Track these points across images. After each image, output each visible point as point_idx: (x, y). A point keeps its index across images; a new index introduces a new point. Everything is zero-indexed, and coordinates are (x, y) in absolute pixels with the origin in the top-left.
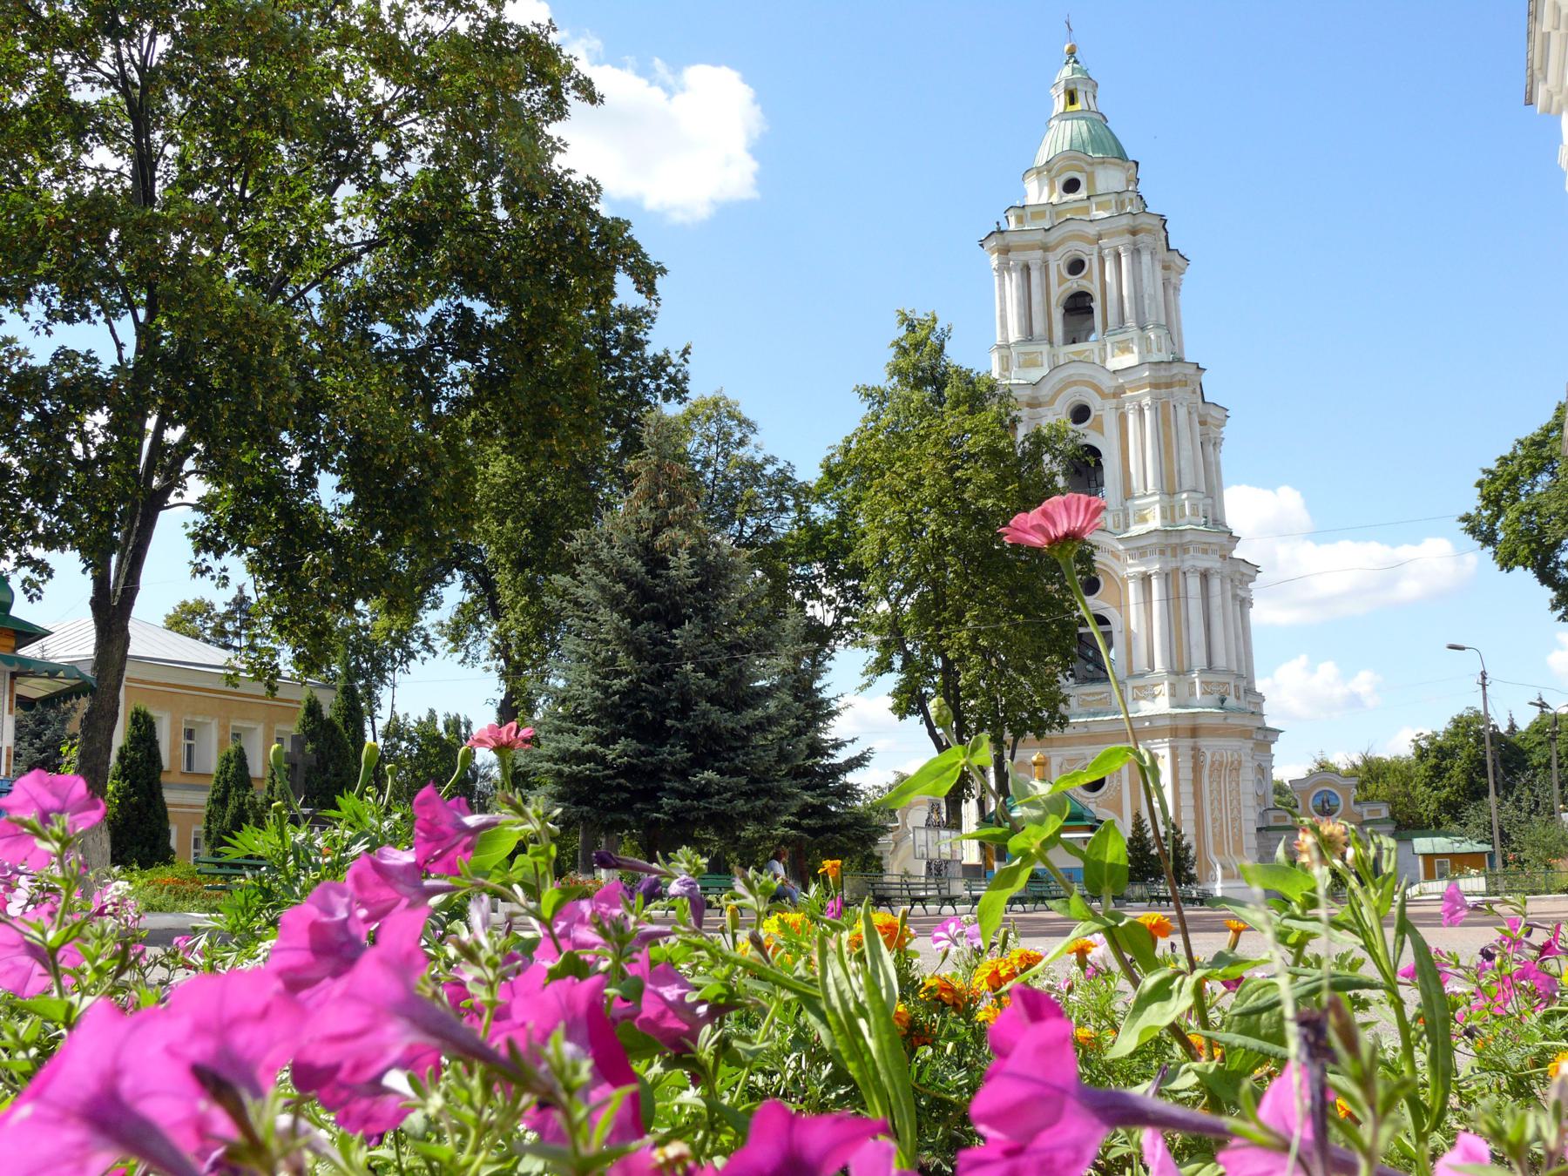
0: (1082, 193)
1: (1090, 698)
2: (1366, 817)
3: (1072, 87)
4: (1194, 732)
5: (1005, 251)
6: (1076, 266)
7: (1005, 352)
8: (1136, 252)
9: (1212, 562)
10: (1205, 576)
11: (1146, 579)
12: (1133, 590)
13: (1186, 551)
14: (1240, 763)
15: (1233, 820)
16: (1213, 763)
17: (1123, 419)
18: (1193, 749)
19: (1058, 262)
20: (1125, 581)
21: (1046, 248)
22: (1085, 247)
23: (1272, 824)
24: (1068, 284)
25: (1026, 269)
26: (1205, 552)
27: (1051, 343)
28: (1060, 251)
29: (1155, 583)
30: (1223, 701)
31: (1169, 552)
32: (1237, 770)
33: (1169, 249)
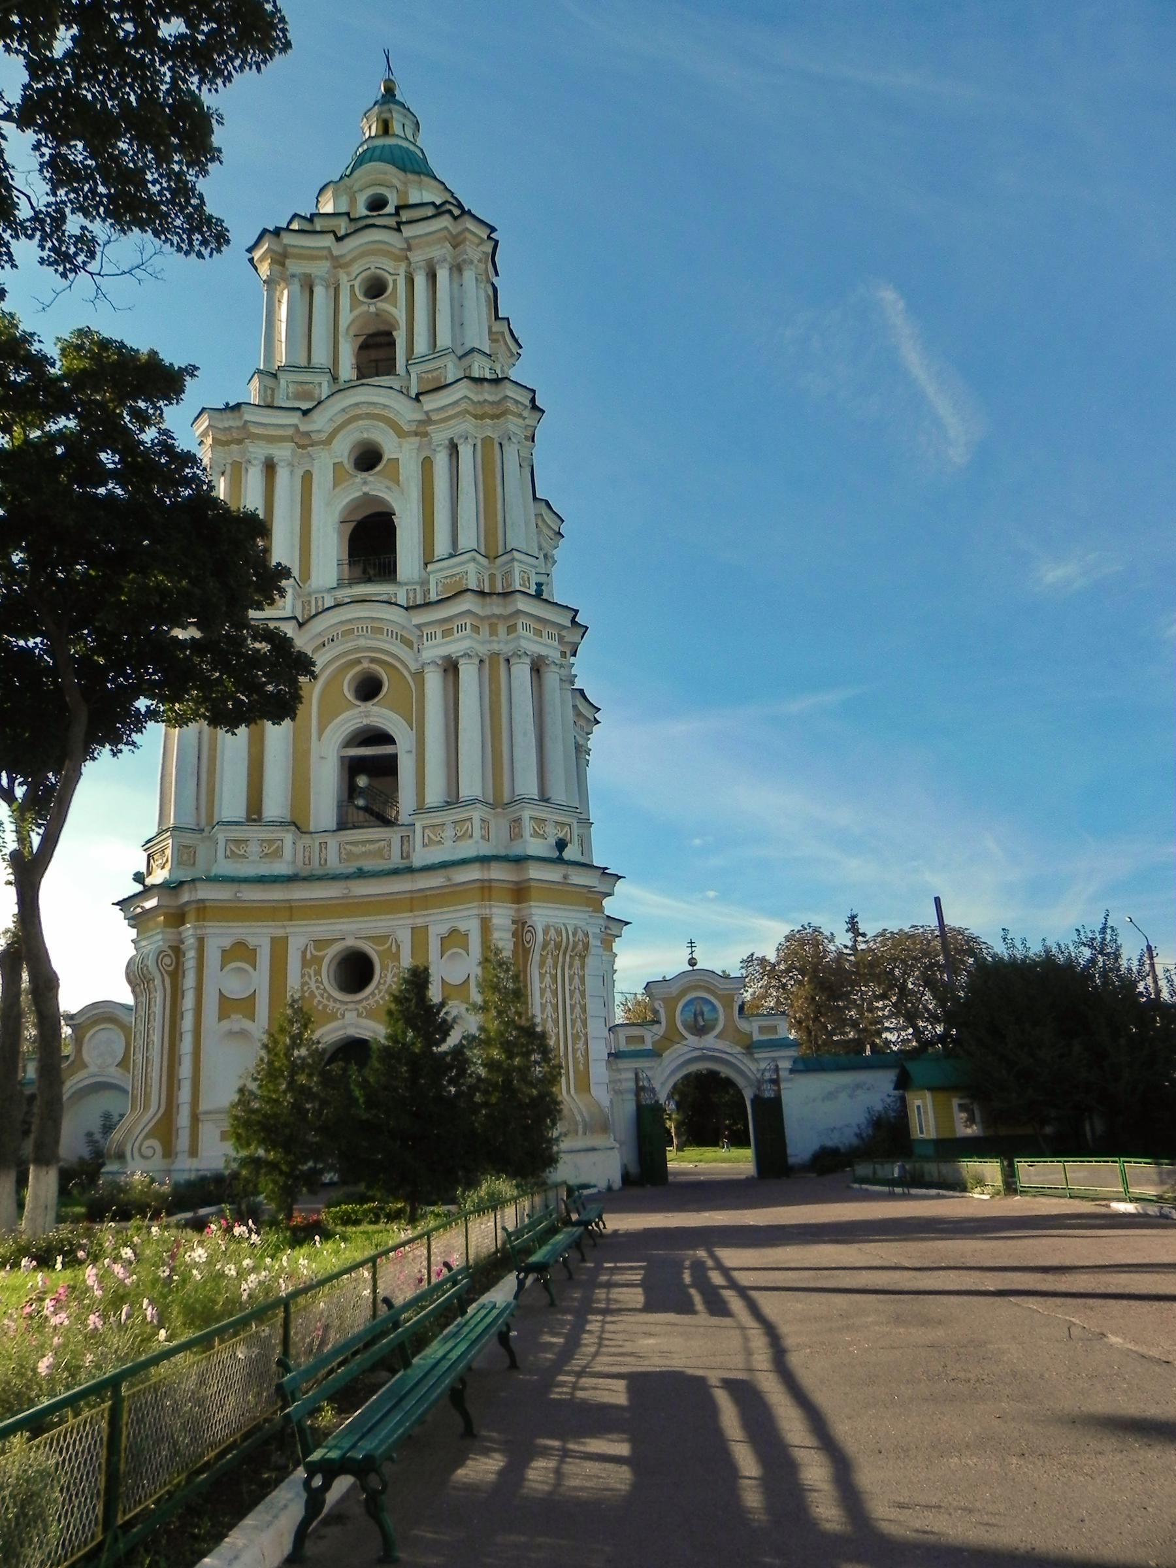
0: (390, 209)
1: (353, 849)
2: (757, 1037)
3: (386, 115)
4: (520, 893)
5: (280, 259)
6: (376, 288)
7: (269, 382)
8: (457, 269)
9: (549, 648)
10: (537, 669)
11: (451, 668)
12: (434, 682)
13: (511, 629)
14: (586, 946)
15: (576, 1037)
16: (545, 945)
17: (427, 465)
18: (514, 922)
19: (351, 281)
20: (419, 676)
21: (338, 263)
22: (389, 265)
23: (623, 1047)
24: (364, 308)
25: (309, 287)
26: (538, 633)
27: (335, 379)
28: (356, 268)
29: (468, 673)
30: (561, 845)
31: (485, 630)
32: (583, 958)
33: (497, 318)
